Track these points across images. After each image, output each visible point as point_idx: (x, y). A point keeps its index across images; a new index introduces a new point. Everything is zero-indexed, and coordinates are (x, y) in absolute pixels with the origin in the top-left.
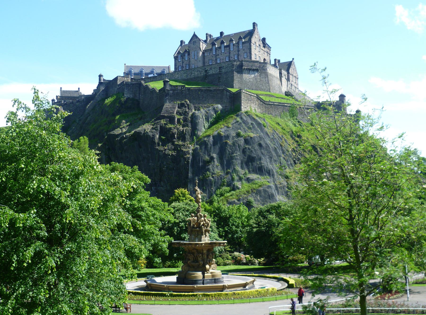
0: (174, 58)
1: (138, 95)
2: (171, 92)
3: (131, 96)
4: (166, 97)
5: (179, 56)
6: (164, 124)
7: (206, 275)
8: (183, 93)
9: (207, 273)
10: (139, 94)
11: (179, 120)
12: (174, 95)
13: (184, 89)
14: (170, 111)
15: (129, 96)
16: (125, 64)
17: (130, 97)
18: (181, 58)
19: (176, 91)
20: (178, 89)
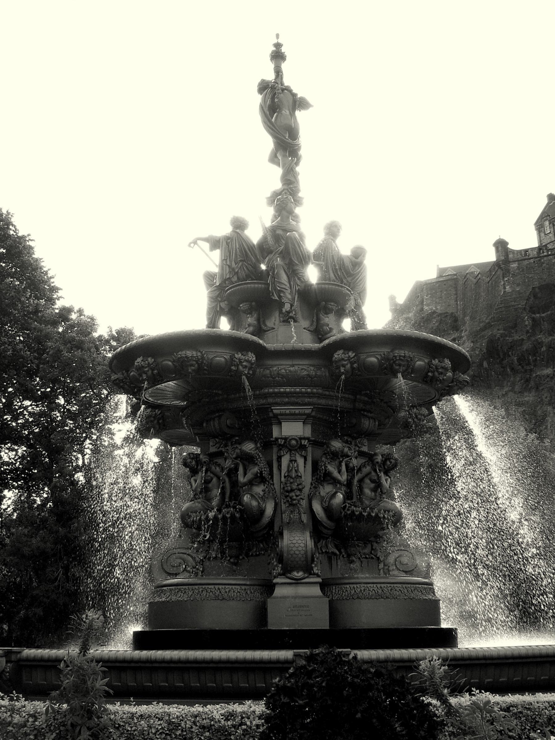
0: (536, 229)
1: (453, 302)
2: (514, 265)
3: (438, 307)
4: (504, 278)
5: (547, 223)
6: (501, 334)
7: (279, 591)
8: (543, 263)
9: (297, 582)
10: (457, 301)
11: (536, 323)
12: (523, 271)
13: (545, 254)
14: (513, 306)
15: (434, 308)
16: (438, 266)
17: (437, 309)
18: (551, 225)
19: (526, 262)
20: (530, 256)
